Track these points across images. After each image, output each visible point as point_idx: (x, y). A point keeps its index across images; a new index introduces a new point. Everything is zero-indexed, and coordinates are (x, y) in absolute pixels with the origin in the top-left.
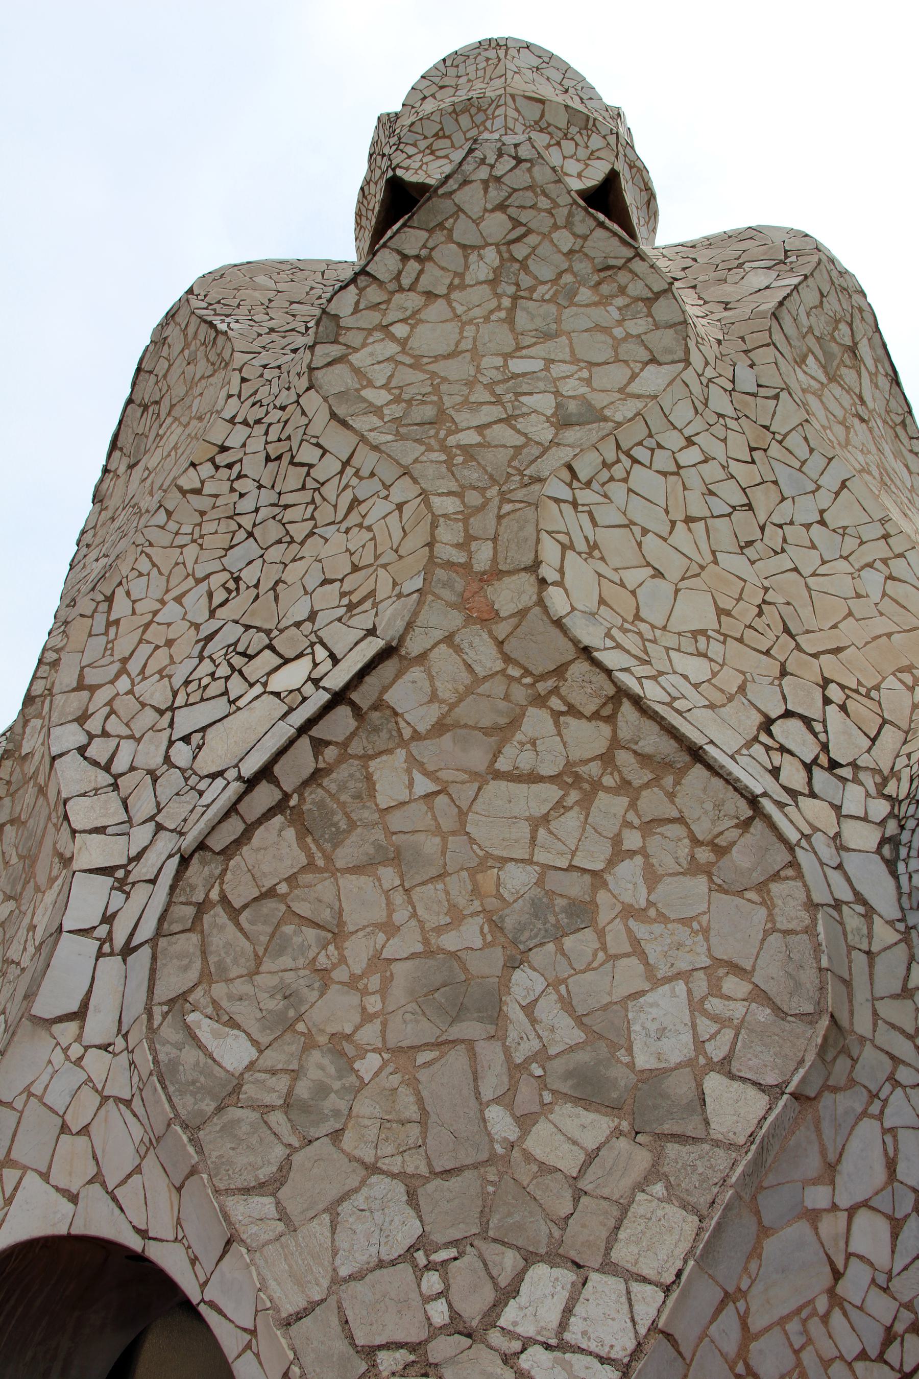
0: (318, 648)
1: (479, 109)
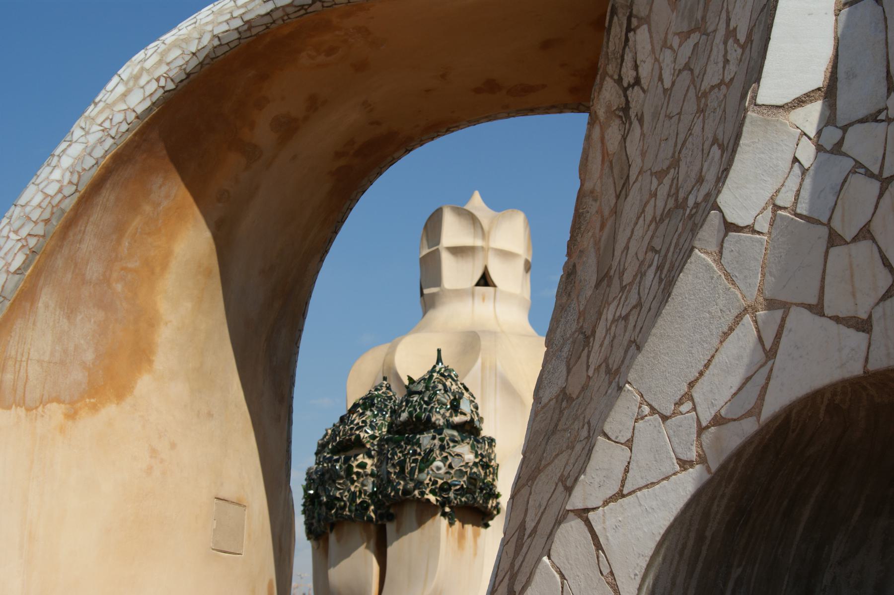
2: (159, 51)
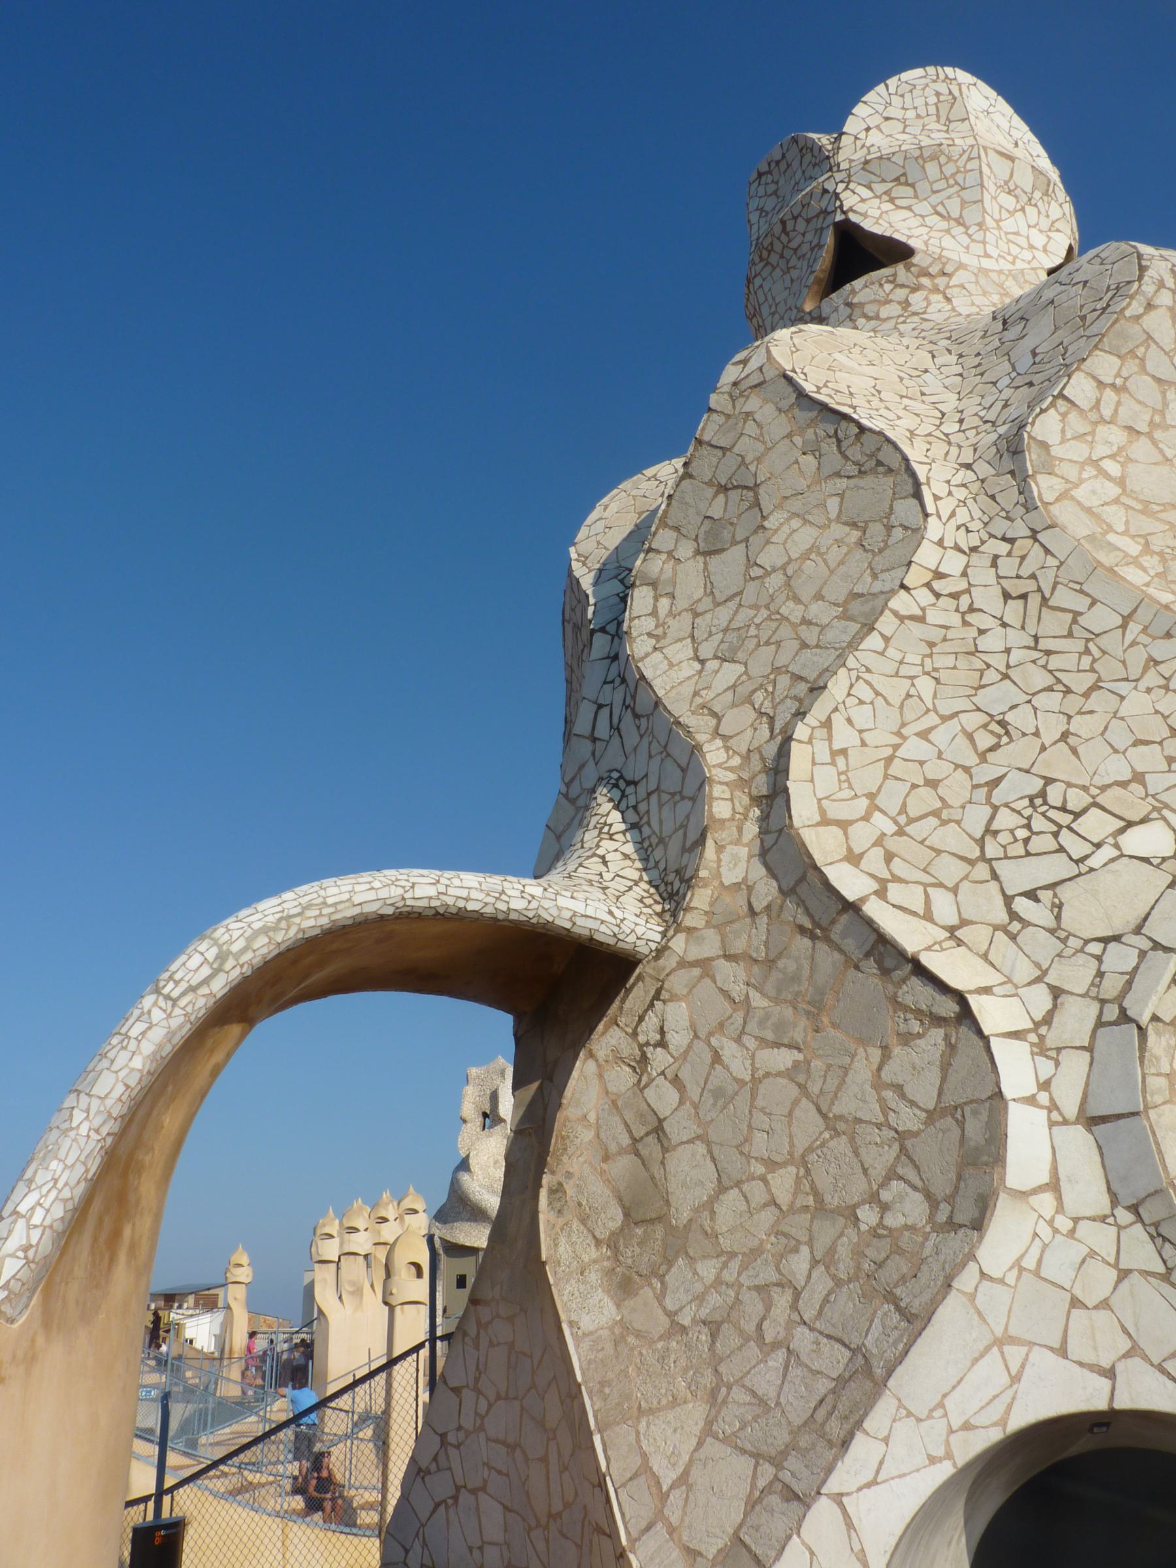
0: (1166, 812)
1: (949, 159)
2: (246, 935)
